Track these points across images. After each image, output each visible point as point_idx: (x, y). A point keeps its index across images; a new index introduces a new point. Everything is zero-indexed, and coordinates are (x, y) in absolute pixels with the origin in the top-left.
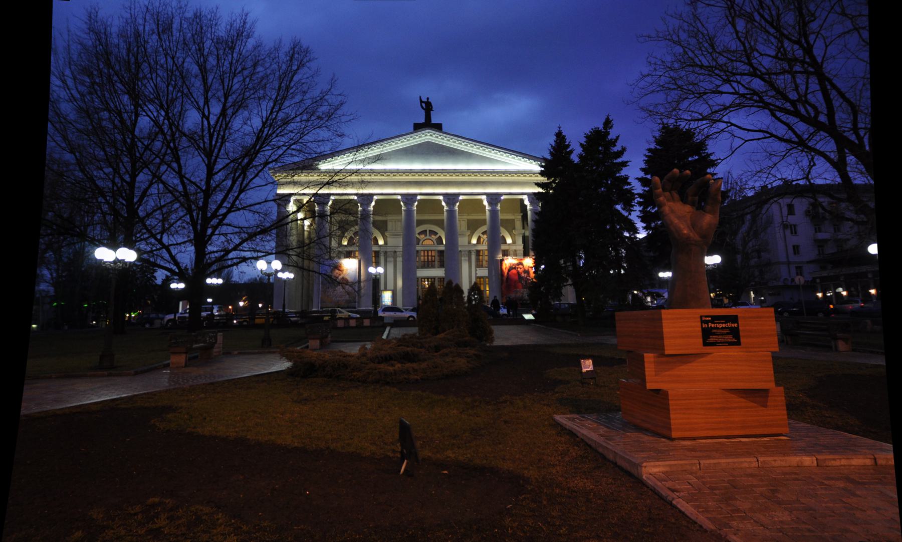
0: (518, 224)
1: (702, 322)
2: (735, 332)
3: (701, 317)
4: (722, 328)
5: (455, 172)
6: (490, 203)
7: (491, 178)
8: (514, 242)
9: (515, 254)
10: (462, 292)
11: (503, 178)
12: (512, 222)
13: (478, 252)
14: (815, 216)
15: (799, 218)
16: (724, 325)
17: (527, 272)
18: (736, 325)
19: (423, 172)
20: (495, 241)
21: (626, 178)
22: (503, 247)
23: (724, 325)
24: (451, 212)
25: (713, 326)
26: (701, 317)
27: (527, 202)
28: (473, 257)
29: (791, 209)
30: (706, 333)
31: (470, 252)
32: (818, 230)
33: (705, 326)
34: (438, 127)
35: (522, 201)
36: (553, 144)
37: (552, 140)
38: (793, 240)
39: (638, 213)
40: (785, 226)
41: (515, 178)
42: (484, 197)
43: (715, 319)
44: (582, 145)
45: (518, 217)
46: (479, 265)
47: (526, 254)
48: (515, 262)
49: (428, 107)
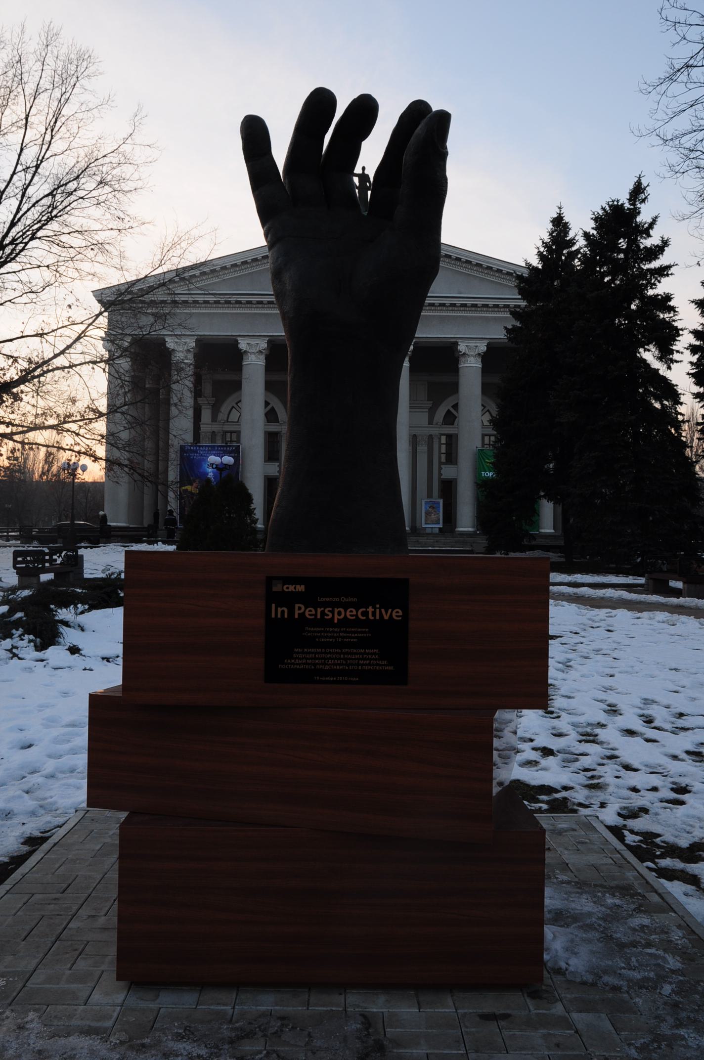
1: (272, 598)
2: (392, 641)
3: (269, 581)
4: (345, 622)
10: (249, 498)
16: (350, 613)
18: (397, 614)
21: (668, 297)
23: (350, 613)
25: (309, 613)
26: (269, 581)
30: (282, 638)
31: (431, 437)
33: (279, 612)
36: (547, 238)
37: (543, 232)
39: (689, 368)
43: (319, 589)
44: (586, 235)
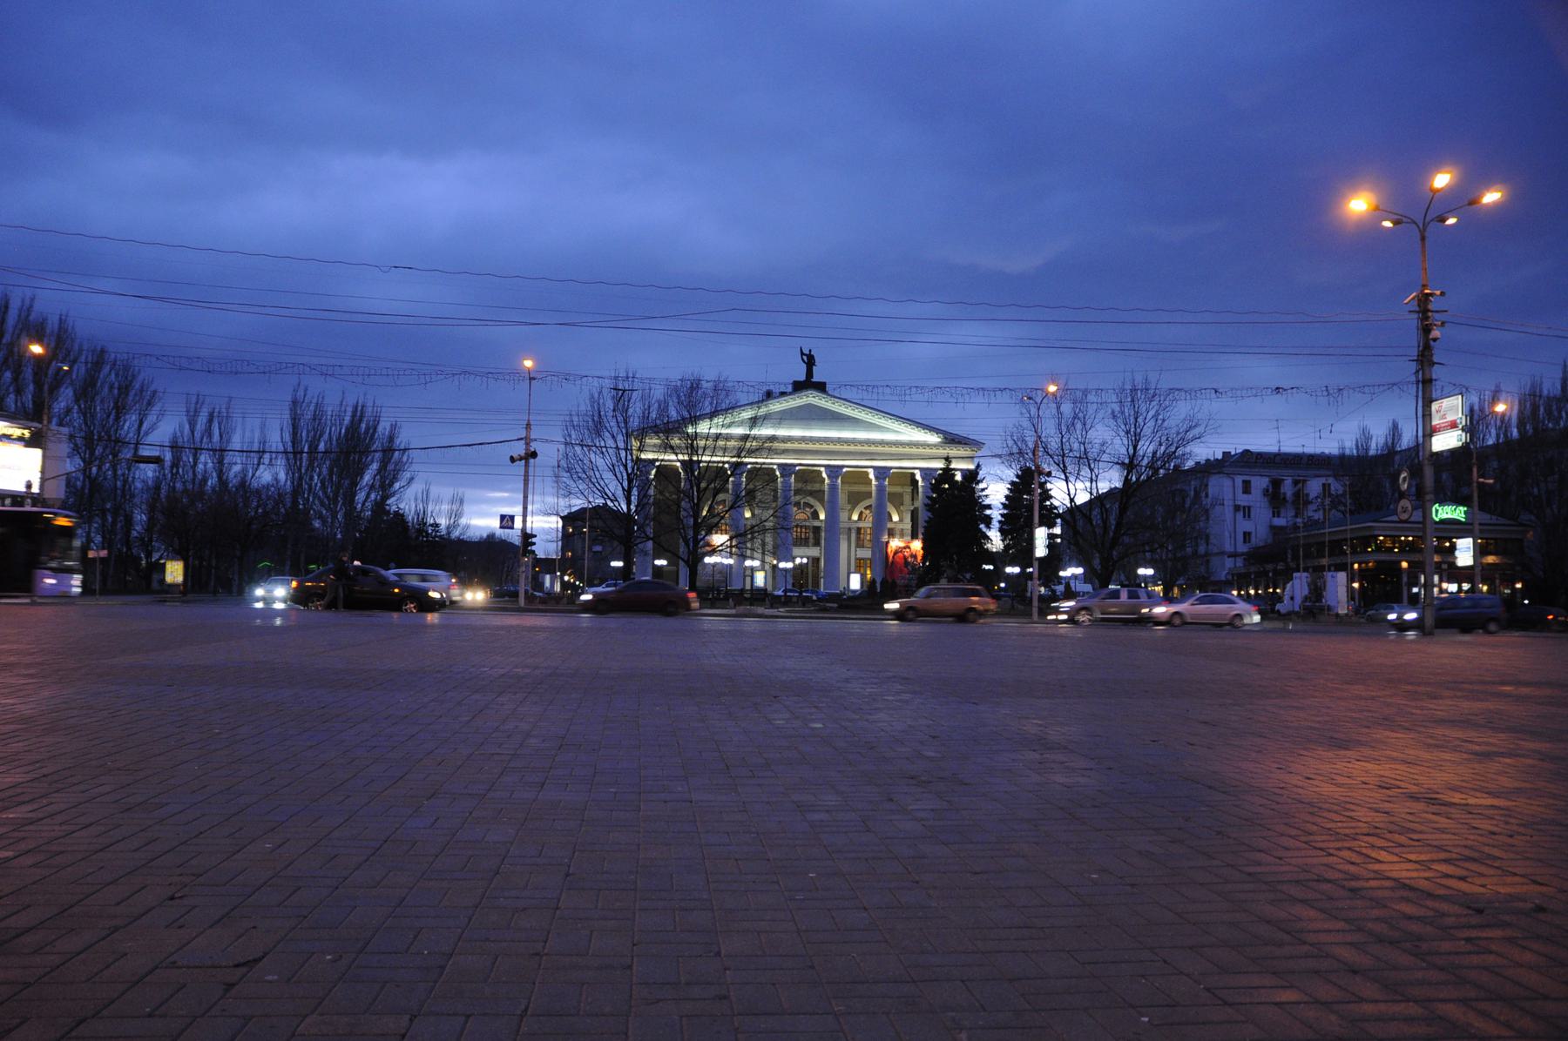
0: (907, 498)
5: (839, 441)
6: (877, 478)
7: (880, 449)
8: (901, 520)
9: (902, 535)
11: (894, 450)
12: (901, 495)
13: (859, 529)
14: (1274, 497)
15: (1256, 499)
17: (915, 556)
19: (803, 439)
20: (881, 518)
22: (889, 525)
24: (833, 487)
27: (918, 477)
28: (853, 536)
29: (1247, 488)
32: (1276, 514)
34: (821, 387)
35: (913, 475)
38: (1247, 526)
40: (1237, 508)
41: (907, 450)
42: (871, 471)
45: (909, 489)
46: (860, 545)
47: (914, 536)
48: (902, 544)
49: (810, 361)
